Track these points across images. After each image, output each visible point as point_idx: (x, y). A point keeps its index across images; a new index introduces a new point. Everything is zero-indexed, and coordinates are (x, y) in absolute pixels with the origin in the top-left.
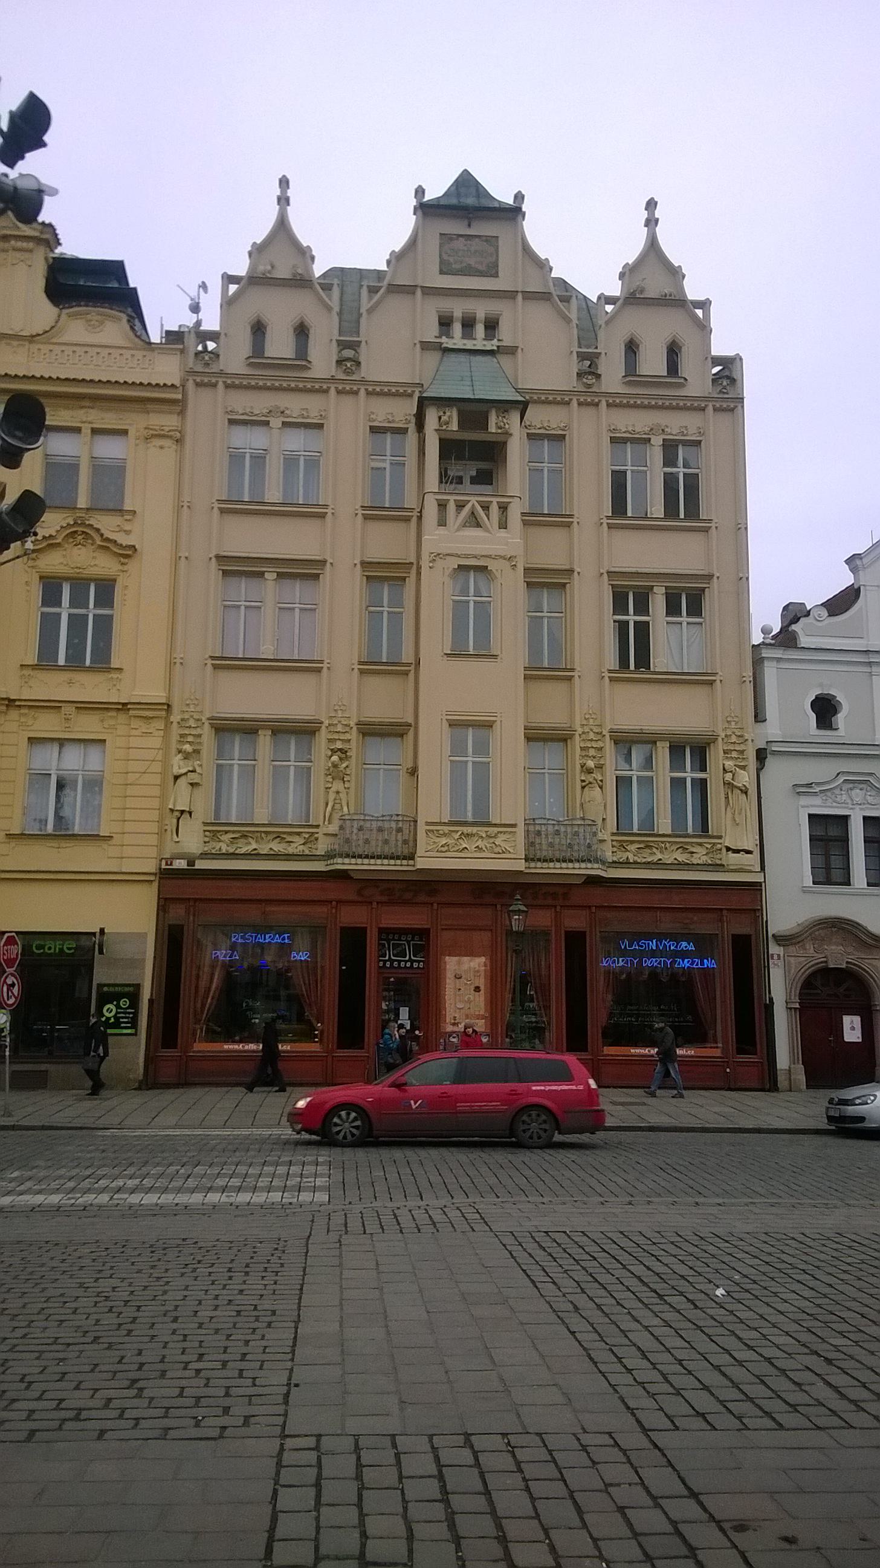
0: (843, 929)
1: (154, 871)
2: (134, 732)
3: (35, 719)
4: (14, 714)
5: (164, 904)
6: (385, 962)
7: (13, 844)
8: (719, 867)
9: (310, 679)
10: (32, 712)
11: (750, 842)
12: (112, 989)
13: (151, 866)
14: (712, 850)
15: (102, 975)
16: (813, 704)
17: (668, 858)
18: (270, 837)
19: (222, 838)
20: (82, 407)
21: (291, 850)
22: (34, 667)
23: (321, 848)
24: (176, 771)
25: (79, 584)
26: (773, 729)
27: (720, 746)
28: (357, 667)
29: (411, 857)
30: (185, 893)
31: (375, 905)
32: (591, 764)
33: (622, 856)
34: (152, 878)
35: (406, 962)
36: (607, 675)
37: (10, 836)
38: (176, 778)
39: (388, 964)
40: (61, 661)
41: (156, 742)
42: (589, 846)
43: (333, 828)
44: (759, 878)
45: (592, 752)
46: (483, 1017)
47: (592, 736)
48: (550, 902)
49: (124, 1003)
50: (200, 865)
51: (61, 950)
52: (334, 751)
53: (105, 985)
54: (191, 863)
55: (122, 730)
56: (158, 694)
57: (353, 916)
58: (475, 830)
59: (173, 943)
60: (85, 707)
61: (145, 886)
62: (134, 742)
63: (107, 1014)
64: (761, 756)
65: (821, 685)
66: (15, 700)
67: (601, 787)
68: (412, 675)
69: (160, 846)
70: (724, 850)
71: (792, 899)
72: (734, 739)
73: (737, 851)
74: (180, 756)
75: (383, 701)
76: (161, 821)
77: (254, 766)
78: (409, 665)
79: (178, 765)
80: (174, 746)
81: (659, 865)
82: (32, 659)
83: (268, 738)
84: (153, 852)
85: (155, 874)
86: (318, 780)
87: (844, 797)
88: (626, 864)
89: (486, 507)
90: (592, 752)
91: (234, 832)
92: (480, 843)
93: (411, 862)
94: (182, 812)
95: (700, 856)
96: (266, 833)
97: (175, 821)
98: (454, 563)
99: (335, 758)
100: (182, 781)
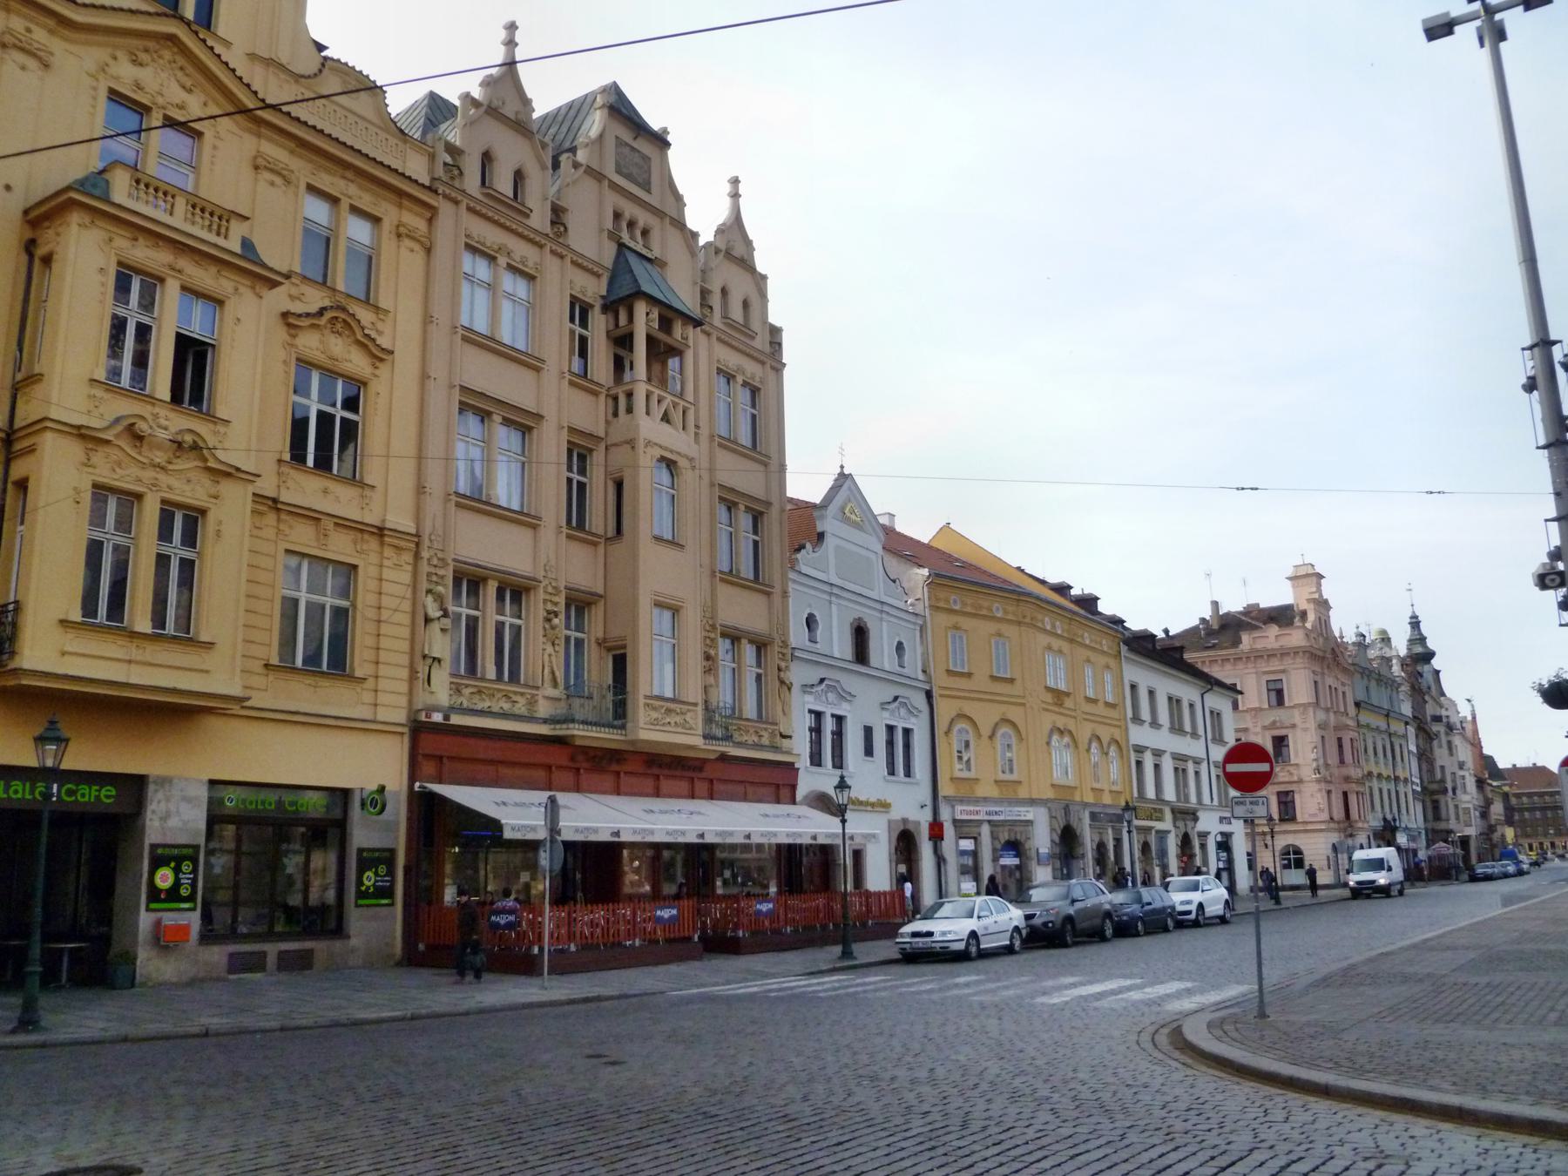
1: (403, 721)
7: (271, 678)
14: (772, 734)
20: (344, 177)
23: (543, 709)
25: (330, 374)
34: (400, 729)
41: (406, 577)
49: (382, 869)
50: (456, 720)
54: (447, 718)
60: (343, 524)
61: (398, 738)
89: (675, 405)
98: (658, 453)
100: (436, 626)
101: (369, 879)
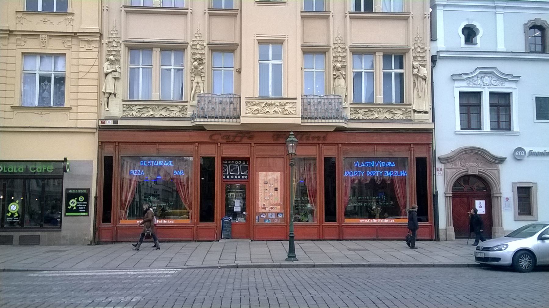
0: (477, 154)
1: (95, 127)
2: (81, 49)
3: (25, 42)
4: (13, 39)
5: (102, 145)
6: (226, 176)
7: (15, 112)
8: (410, 121)
9: (180, 20)
10: (23, 38)
11: (427, 107)
12: (74, 191)
13: (94, 124)
15: (68, 184)
16: (463, 30)
17: (382, 117)
18: (161, 108)
19: (133, 108)
21: (172, 115)
22: (23, 12)
23: (189, 113)
24: (105, 70)
26: (441, 44)
27: (411, 54)
28: (207, 12)
29: (238, 117)
30: (113, 139)
31: (219, 144)
32: (339, 65)
33: (356, 116)
35: (238, 175)
36: (348, 15)
37: (13, 107)
38: (106, 75)
39: (228, 177)
40: (40, 9)
41: (95, 55)
42: (337, 110)
43: (195, 103)
44: (431, 126)
45: (340, 59)
46: (280, 204)
47: (339, 50)
48: (315, 141)
49: (81, 199)
50: (121, 123)
51: (46, 170)
52: (195, 60)
53: (70, 189)
54: (116, 122)
55: (75, 48)
56: (95, 28)
57: (208, 151)
58: (273, 101)
59: (107, 166)
60: (53, 35)
62: (82, 55)
63: (72, 205)
64: (434, 59)
65: (468, 19)
66: (13, 31)
67: (344, 79)
68: (239, 15)
69: (98, 113)
70: (412, 112)
71: (449, 138)
72: (419, 50)
73: (420, 112)
74: (108, 63)
75: (222, 32)
76: (98, 99)
77: (151, 68)
78: (237, 10)
79: (107, 67)
80: (104, 57)
81: (376, 120)
82: (23, 7)
83: (158, 52)
84: (95, 116)
85: (96, 128)
86: (187, 76)
87: (479, 82)
88: (358, 120)
90: (340, 59)
91: (140, 105)
92: (276, 109)
93: (238, 120)
94: (110, 94)
95: (399, 115)
96: (159, 106)
97: (106, 99)
99: (196, 63)
100: (110, 77)
101: (73, 203)
